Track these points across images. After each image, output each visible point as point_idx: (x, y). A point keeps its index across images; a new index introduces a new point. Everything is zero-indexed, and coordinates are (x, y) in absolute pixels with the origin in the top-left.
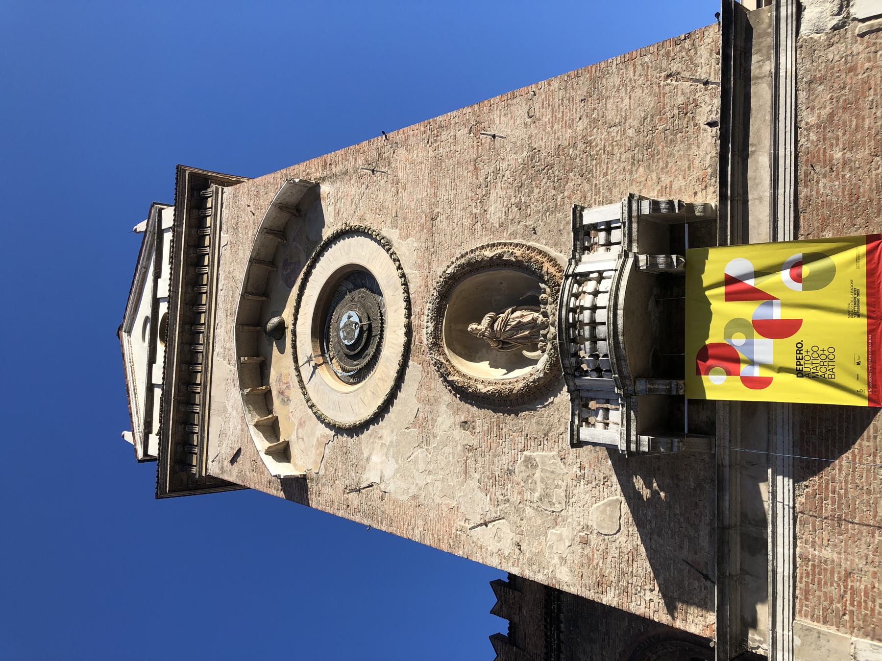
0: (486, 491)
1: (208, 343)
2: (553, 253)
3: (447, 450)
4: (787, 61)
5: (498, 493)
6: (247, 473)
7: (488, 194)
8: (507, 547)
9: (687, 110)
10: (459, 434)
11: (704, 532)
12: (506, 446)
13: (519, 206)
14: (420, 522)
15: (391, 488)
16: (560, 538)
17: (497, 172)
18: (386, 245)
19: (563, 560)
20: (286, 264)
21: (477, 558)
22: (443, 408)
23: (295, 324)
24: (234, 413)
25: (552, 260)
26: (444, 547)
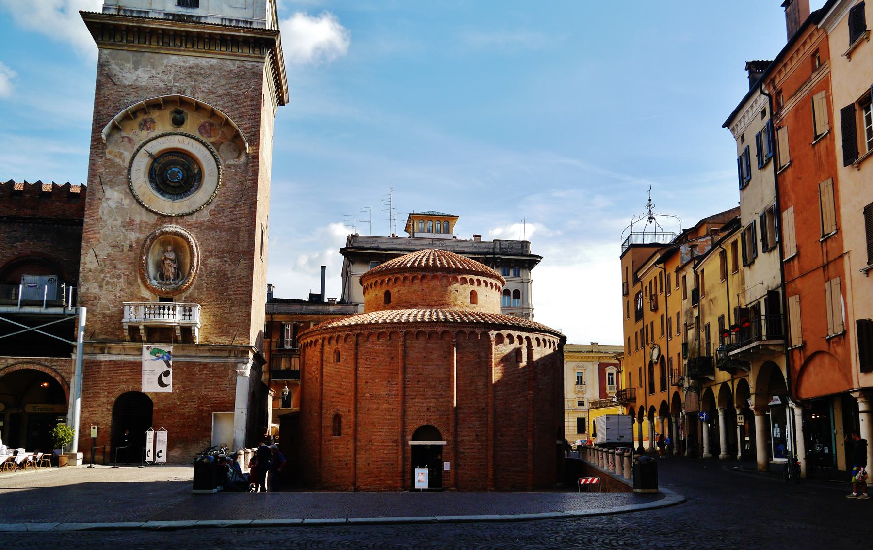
0: (108, 256)
1: (175, 50)
2: (192, 288)
3: (122, 237)
4: (232, 360)
5: (107, 262)
6: (103, 92)
7: (219, 258)
8: (88, 266)
9: (226, 334)
10: (128, 242)
11: (104, 337)
12: (125, 266)
13: (212, 272)
14: (91, 222)
15: (104, 205)
16: (95, 288)
17: (226, 262)
18: (208, 203)
19: (88, 289)
20: (211, 125)
21: (83, 252)
22: (138, 235)
23: (182, 134)
24: (135, 78)
25: (188, 287)
26: (84, 235)
